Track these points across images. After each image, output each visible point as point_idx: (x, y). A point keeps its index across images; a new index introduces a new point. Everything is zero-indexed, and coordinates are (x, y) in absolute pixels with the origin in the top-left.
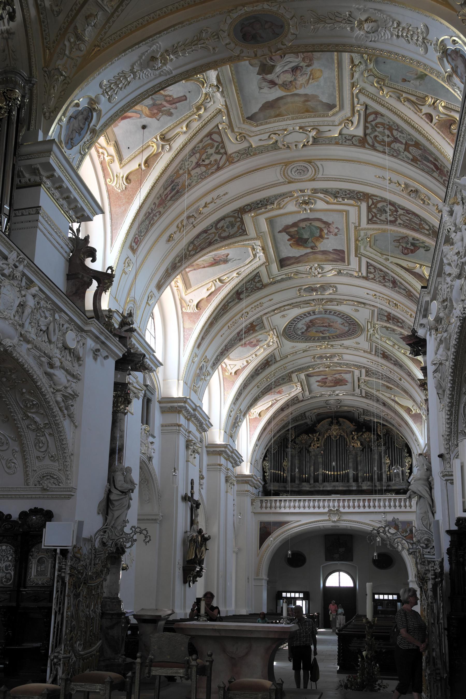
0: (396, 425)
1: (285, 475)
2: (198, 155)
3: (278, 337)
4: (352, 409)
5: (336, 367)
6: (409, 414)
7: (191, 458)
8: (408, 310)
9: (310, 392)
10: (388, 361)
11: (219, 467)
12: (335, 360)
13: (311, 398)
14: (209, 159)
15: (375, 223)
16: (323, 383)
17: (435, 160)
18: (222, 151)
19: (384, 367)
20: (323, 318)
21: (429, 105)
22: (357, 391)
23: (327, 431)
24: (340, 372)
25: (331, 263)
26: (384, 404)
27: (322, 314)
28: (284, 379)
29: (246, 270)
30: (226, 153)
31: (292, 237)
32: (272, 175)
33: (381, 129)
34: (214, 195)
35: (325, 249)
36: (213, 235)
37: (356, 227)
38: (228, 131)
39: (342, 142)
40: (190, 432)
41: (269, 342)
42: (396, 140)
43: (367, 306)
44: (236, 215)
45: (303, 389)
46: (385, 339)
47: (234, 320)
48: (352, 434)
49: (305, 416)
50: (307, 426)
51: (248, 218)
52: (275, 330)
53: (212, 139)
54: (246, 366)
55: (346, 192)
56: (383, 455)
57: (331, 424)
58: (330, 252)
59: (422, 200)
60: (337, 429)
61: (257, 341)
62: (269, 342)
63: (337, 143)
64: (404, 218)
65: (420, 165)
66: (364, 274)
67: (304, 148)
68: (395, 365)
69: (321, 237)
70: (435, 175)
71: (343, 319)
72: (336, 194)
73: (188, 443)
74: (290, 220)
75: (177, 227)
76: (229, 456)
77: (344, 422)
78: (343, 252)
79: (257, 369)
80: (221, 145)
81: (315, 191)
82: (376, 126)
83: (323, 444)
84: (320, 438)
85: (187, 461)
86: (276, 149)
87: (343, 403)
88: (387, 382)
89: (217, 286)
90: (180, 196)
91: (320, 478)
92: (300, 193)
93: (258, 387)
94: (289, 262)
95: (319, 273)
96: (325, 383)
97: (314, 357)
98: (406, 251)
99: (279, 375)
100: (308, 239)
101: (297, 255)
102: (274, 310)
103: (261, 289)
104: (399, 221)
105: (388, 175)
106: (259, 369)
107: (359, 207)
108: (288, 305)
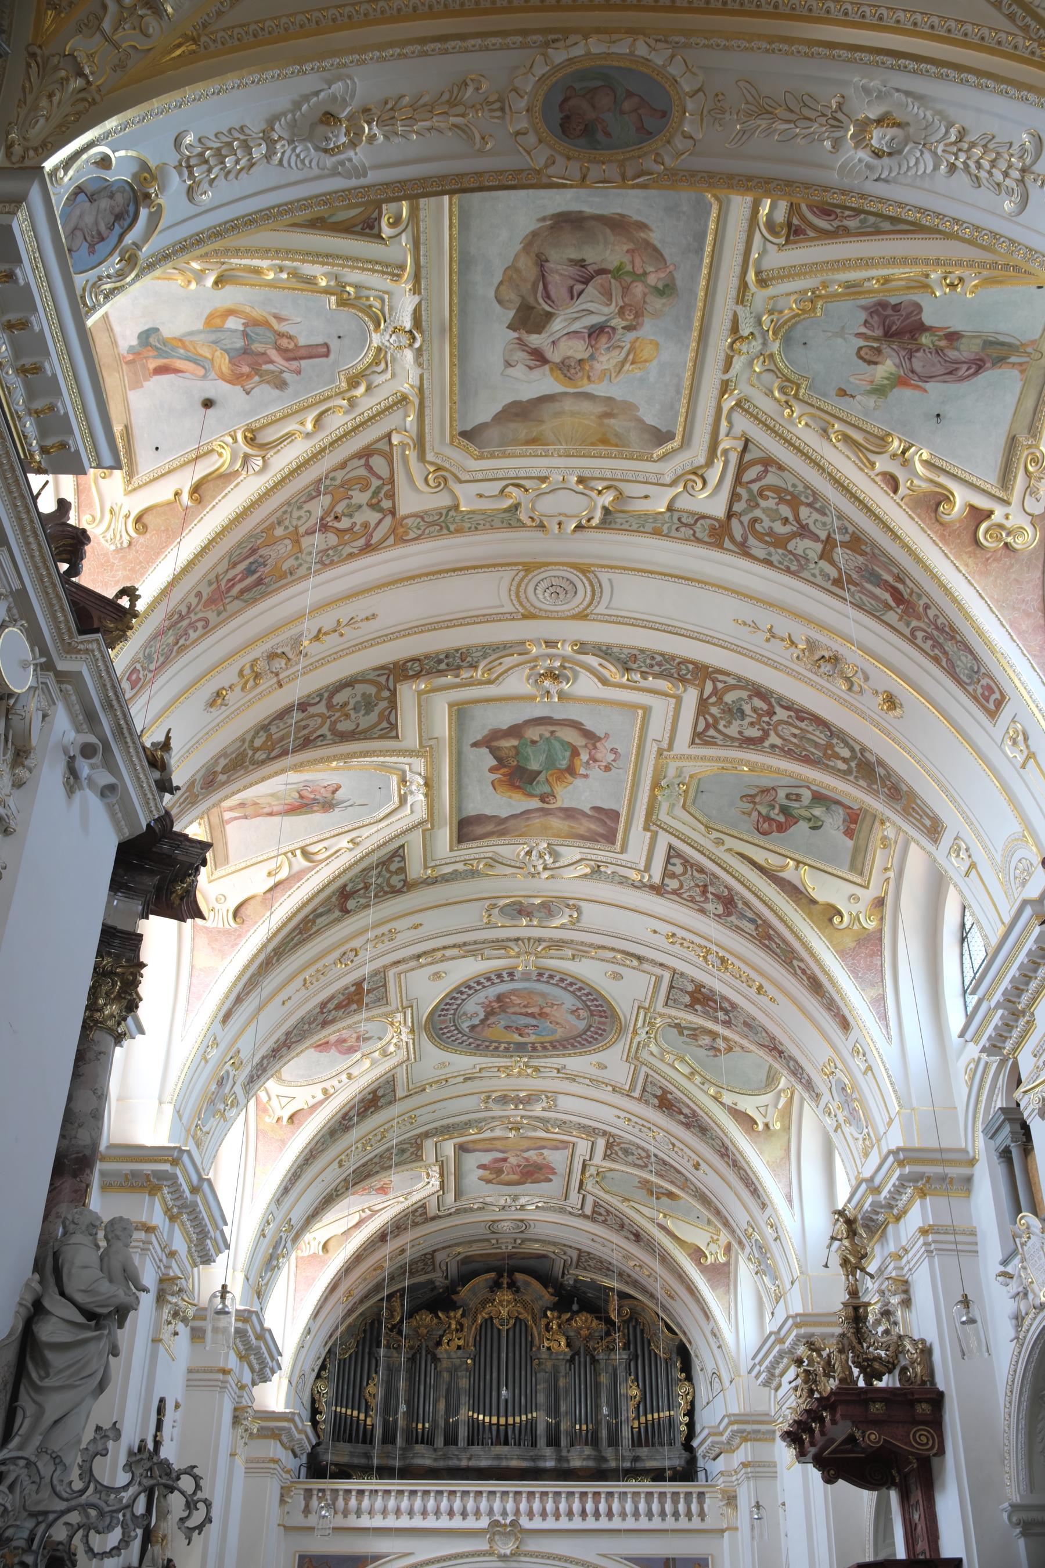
0: (659, 1294)
1: (369, 1421)
2: (325, 500)
3: (412, 1031)
4: (551, 1248)
5: (535, 1128)
6: (699, 1264)
7: (166, 1332)
8: (754, 975)
9: (458, 1195)
10: (671, 1116)
11: (220, 1376)
12: (538, 1110)
13: (458, 1212)
14: (351, 516)
15: (711, 743)
16: (495, 1172)
17: (899, 579)
18: (386, 504)
19: (660, 1133)
20: (531, 993)
21: (894, 456)
22: (575, 1198)
23: (484, 1303)
24: (540, 1145)
25: (581, 843)
26: (637, 1237)
27: (529, 980)
28: (403, 1151)
29: (374, 837)
30: (393, 512)
31: (501, 762)
32: (489, 592)
33: (771, 503)
34: (344, 612)
35: (573, 805)
36: (319, 720)
37: (660, 753)
38: (411, 454)
39: (670, 529)
40: (172, 1254)
41: (389, 1043)
42: (804, 531)
43: (646, 966)
44: (383, 679)
45: (442, 1183)
46: (673, 1057)
47: (319, 965)
48: (546, 1316)
49: (433, 1263)
50: (432, 1290)
51: (408, 693)
52: (409, 1011)
53: (368, 467)
54: (321, 1102)
55: (653, 658)
56: (621, 1373)
57: (496, 1285)
58: (584, 814)
59: (847, 679)
60: (509, 1302)
61: (358, 1038)
62: (389, 1043)
63: (657, 533)
64: (787, 731)
65: (853, 595)
66: (657, 879)
67: (579, 535)
68: (687, 1126)
69: (571, 770)
70: (892, 617)
71: (579, 997)
72: (628, 661)
73: (165, 1286)
74: (506, 718)
75: (241, 673)
76: (249, 1347)
77: (527, 1284)
78: (615, 815)
79: (346, 1114)
80: (387, 488)
81: (583, 647)
82: (761, 494)
83: (471, 1341)
84: (465, 1321)
85: (156, 1341)
86: (510, 526)
87: (532, 1230)
88: (659, 1175)
89: (296, 868)
90: (264, 595)
91: (463, 1433)
92: (544, 650)
93: (340, 1165)
94: (479, 830)
95: (545, 868)
96: (499, 1172)
97: (489, 1097)
98: (766, 825)
99: (394, 1138)
100: (539, 773)
101: (504, 814)
102: (419, 956)
103: (399, 892)
104: (773, 739)
105: (766, 618)
107: (679, 700)
108: (454, 946)
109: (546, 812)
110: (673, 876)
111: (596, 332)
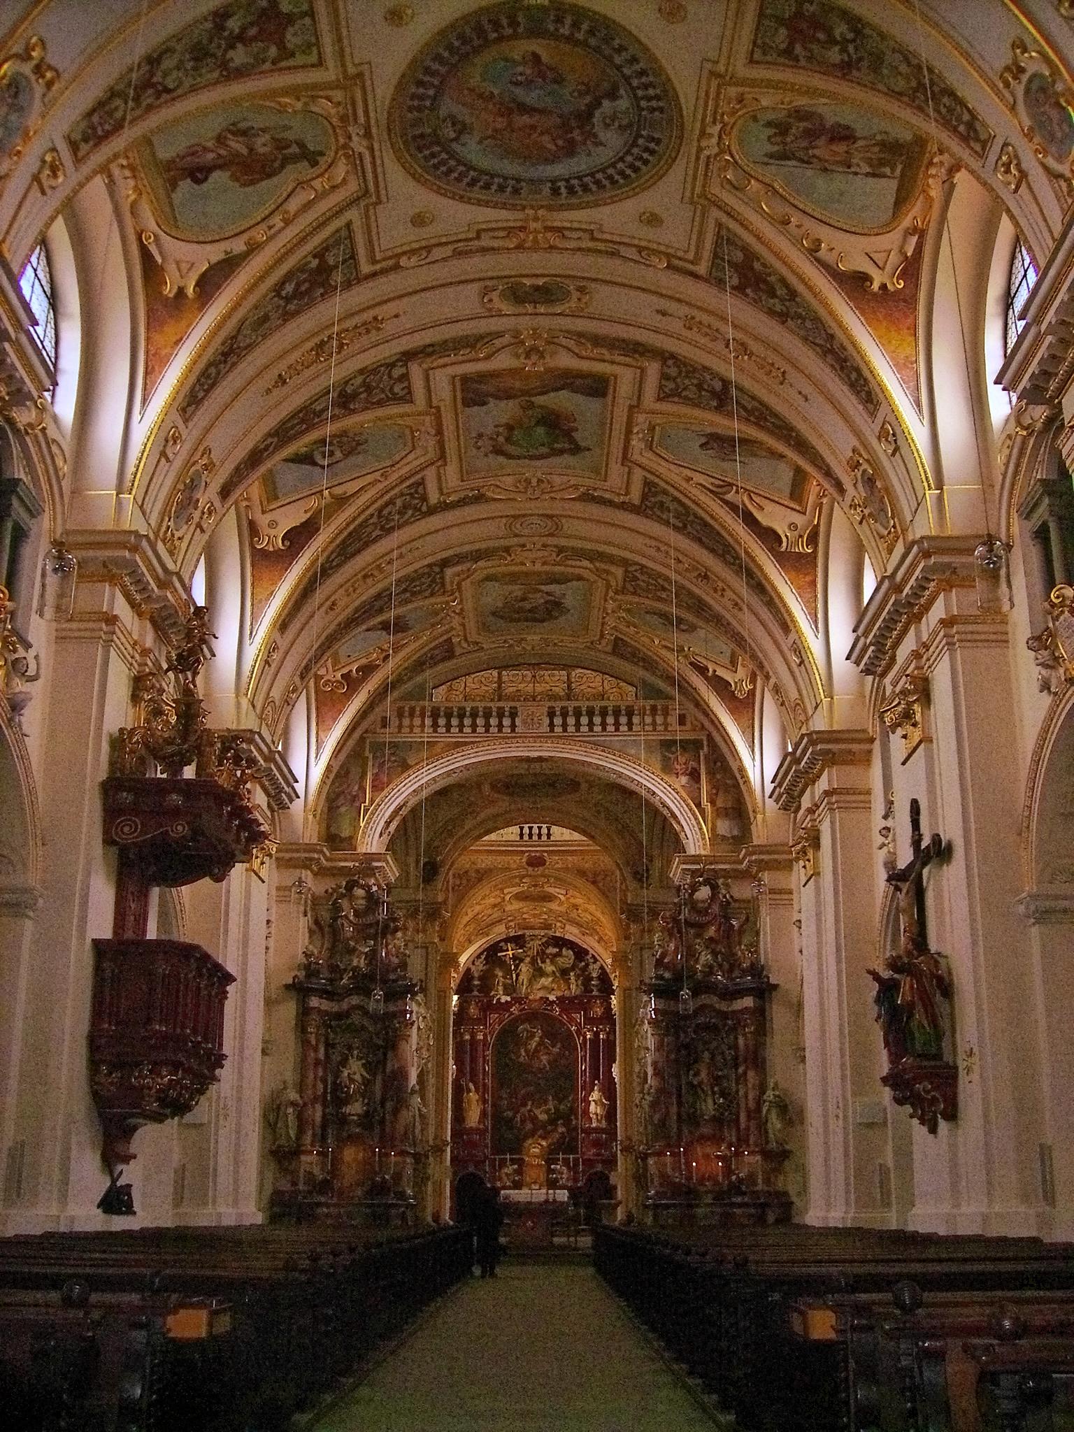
30: (626, 571)
31: (568, 434)
35: (503, 404)
51: (635, 496)
52: (698, 190)
58: (492, 396)
71: (459, 162)
78: (467, 403)
101: (564, 394)
103: (673, 356)
106: (834, 55)
111: (523, 599)
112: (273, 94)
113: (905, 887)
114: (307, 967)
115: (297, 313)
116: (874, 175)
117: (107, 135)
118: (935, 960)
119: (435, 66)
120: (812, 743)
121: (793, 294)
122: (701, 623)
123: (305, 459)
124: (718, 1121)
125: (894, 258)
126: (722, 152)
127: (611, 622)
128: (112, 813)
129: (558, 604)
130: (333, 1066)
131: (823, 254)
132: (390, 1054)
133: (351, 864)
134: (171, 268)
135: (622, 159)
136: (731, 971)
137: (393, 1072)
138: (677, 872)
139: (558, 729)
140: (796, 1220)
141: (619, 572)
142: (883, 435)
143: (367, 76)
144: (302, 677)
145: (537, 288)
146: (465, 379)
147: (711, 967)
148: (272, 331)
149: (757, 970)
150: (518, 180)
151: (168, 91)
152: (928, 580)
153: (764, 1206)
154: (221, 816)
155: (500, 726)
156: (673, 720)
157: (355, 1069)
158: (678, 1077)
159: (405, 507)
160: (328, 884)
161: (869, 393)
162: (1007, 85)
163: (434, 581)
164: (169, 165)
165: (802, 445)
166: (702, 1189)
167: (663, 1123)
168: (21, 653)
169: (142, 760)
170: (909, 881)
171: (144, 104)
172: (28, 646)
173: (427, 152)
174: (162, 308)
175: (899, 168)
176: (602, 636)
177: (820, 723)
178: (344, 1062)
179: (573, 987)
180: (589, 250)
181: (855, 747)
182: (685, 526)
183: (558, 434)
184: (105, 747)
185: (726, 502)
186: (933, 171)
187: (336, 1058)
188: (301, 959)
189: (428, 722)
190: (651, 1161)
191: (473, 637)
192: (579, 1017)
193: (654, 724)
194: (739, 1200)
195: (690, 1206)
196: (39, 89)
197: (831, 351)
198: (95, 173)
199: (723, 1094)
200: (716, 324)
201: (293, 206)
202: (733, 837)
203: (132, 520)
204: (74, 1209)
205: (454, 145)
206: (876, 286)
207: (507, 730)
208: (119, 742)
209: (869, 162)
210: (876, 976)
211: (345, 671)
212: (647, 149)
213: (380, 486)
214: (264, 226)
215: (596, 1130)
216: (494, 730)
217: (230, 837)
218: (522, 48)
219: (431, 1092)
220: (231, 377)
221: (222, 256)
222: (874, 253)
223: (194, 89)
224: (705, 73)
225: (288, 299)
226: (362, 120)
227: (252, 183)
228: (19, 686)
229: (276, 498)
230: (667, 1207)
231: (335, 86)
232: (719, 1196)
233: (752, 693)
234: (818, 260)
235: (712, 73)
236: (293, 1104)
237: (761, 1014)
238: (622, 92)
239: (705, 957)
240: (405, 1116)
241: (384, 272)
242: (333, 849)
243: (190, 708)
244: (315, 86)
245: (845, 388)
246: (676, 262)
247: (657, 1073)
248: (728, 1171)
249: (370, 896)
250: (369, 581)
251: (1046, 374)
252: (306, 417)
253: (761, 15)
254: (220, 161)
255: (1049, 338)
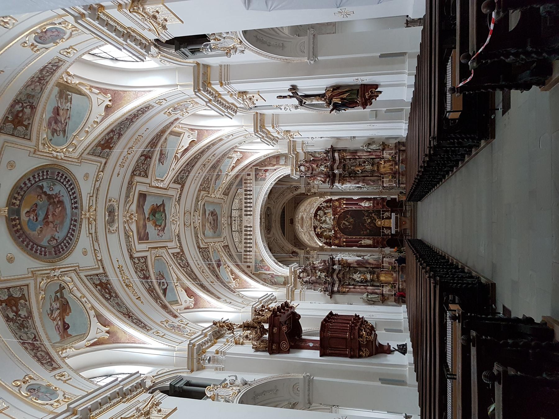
27: (72, 215)
31: (158, 207)
69: (156, 225)
71: (65, 239)
94: (141, 200)
103: (133, 172)
106: (28, 111)
109: (144, 220)
110: (139, 260)
112: (37, 301)
113: (304, 101)
114: (325, 291)
115: (116, 293)
116: (71, 102)
117: (50, 358)
118: (327, 90)
119: (30, 247)
120: (257, 132)
121: (112, 131)
122: (218, 168)
123: (165, 291)
124: (373, 165)
125: (100, 97)
126: (62, 152)
127: (218, 196)
128: (279, 351)
129: (212, 213)
130: (356, 283)
131: (98, 120)
132: (351, 266)
133: (293, 278)
134: (99, 336)
135: (65, 185)
136: (326, 160)
137: (357, 264)
138: (296, 176)
139: (251, 213)
140: (404, 140)
141: (203, 192)
142: (160, 103)
143: (32, 269)
144: (235, 292)
145: (109, 215)
146: (140, 239)
147: (325, 166)
148: (122, 301)
149: (327, 152)
150: (72, 220)
151: (35, 337)
152: (208, 90)
153: (399, 150)
154: (280, 316)
155: (250, 231)
156: (249, 177)
157: (357, 277)
158: (359, 177)
159: (181, 259)
160: (299, 284)
161: (146, 108)
162: (38, 50)
163: (204, 251)
164: (62, 337)
165: (163, 132)
166: (394, 169)
167: (374, 181)
168: (228, 382)
169: (262, 341)
170: (303, 99)
171: (40, 345)
172: (225, 380)
173: (61, 250)
174: (112, 338)
175: (68, 93)
176: (222, 199)
177: (252, 130)
178: (354, 280)
179: (329, 211)
180: (96, 197)
181: (259, 118)
182: (188, 171)
183: (158, 211)
184: (258, 353)
185: (181, 157)
186: (69, 81)
187: (353, 283)
188: (322, 293)
189: (248, 253)
190: (385, 185)
191: (222, 239)
192: (339, 209)
193: (250, 183)
194: (397, 158)
195: (399, 173)
196: (32, 382)
197: (132, 119)
198: (64, 361)
199: (364, 162)
200: (122, 157)
201: (79, 295)
202: (285, 159)
203: (185, 346)
204: (406, 363)
205: (58, 241)
206: (110, 103)
207: (251, 229)
208: (257, 349)
209: (66, 103)
210: (332, 110)
211: (232, 279)
212: (61, 177)
213: (174, 268)
214: (85, 304)
215: (373, 204)
216: (251, 233)
217: (287, 313)
218: (24, 217)
219: (363, 254)
220: (136, 315)
221: (95, 318)
222: (99, 103)
223: (35, 328)
224: (34, 155)
225: (111, 296)
226: (48, 271)
227: (70, 308)
228: (238, 382)
229: (177, 301)
230: (399, 181)
231: (36, 280)
232: (396, 164)
233: (241, 152)
234: (101, 122)
235: (34, 153)
236: (367, 295)
237: (339, 151)
238: (40, 184)
239: (322, 168)
240: (371, 261)
241: (102, 265)
242: (288, 283)
243: (246, 326)
244: (36, 287)
245: (144, 115)
246: (101, 170)
247: (358, 183)
248: (389, 161)
249: (302, 272)
250: (204, 271)
251: (141, 44)
252: (151, 290)
253: (13, 135)
254: (62, 319)
255: (128, 41)
